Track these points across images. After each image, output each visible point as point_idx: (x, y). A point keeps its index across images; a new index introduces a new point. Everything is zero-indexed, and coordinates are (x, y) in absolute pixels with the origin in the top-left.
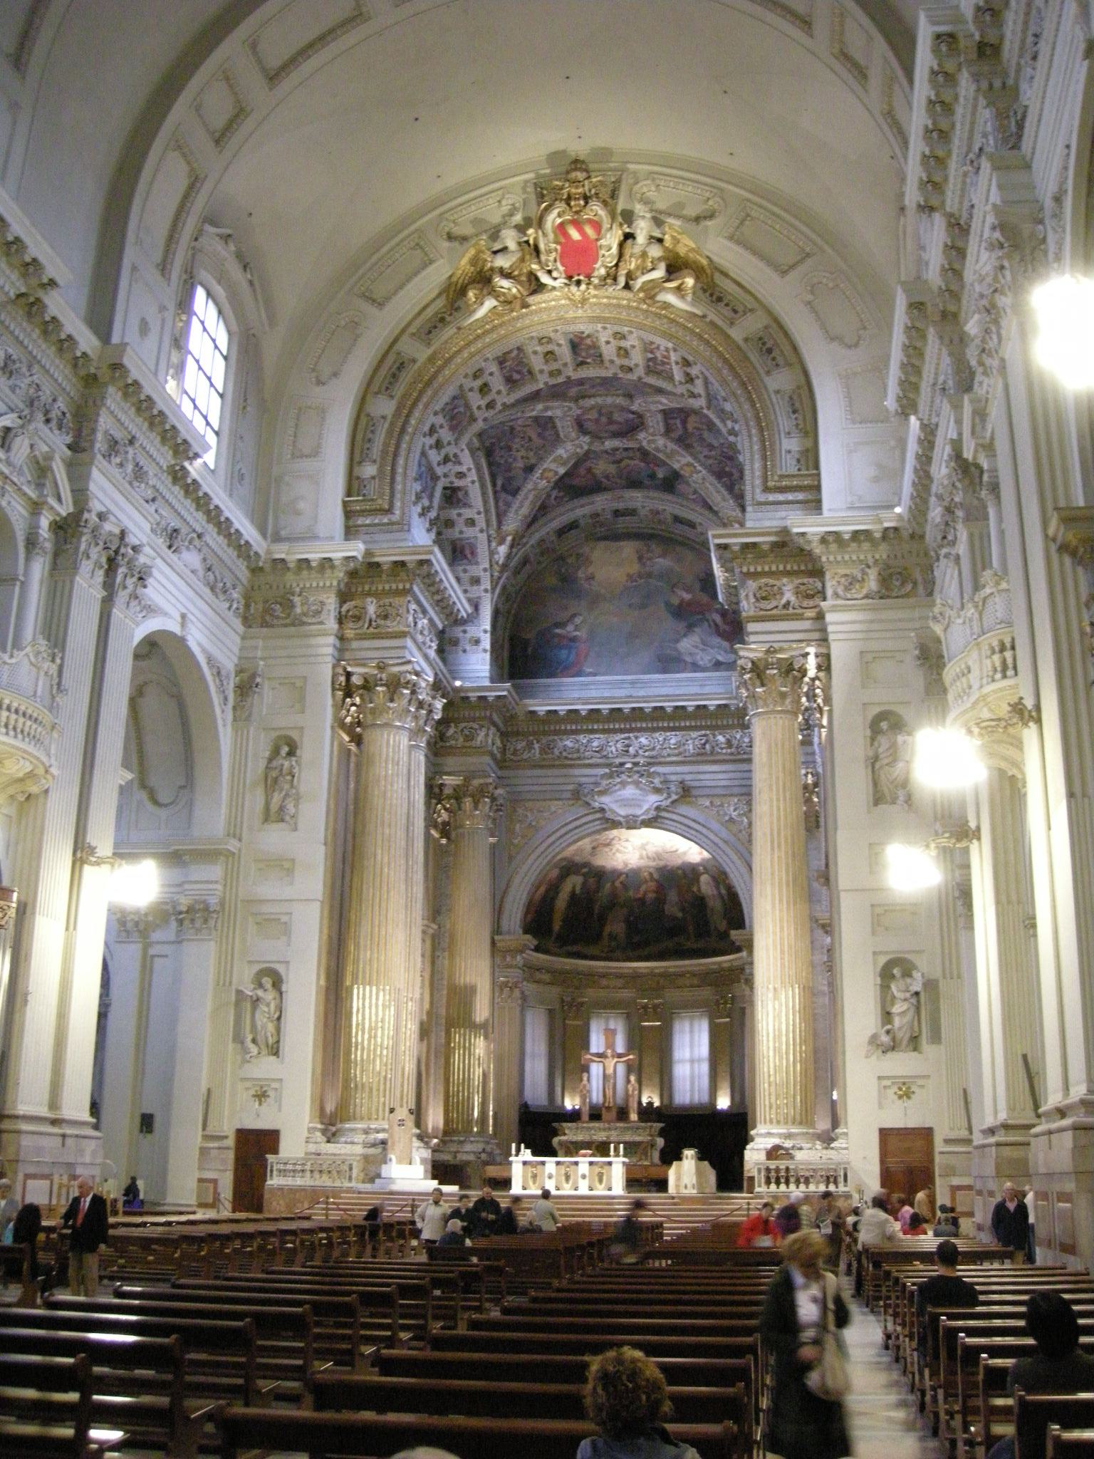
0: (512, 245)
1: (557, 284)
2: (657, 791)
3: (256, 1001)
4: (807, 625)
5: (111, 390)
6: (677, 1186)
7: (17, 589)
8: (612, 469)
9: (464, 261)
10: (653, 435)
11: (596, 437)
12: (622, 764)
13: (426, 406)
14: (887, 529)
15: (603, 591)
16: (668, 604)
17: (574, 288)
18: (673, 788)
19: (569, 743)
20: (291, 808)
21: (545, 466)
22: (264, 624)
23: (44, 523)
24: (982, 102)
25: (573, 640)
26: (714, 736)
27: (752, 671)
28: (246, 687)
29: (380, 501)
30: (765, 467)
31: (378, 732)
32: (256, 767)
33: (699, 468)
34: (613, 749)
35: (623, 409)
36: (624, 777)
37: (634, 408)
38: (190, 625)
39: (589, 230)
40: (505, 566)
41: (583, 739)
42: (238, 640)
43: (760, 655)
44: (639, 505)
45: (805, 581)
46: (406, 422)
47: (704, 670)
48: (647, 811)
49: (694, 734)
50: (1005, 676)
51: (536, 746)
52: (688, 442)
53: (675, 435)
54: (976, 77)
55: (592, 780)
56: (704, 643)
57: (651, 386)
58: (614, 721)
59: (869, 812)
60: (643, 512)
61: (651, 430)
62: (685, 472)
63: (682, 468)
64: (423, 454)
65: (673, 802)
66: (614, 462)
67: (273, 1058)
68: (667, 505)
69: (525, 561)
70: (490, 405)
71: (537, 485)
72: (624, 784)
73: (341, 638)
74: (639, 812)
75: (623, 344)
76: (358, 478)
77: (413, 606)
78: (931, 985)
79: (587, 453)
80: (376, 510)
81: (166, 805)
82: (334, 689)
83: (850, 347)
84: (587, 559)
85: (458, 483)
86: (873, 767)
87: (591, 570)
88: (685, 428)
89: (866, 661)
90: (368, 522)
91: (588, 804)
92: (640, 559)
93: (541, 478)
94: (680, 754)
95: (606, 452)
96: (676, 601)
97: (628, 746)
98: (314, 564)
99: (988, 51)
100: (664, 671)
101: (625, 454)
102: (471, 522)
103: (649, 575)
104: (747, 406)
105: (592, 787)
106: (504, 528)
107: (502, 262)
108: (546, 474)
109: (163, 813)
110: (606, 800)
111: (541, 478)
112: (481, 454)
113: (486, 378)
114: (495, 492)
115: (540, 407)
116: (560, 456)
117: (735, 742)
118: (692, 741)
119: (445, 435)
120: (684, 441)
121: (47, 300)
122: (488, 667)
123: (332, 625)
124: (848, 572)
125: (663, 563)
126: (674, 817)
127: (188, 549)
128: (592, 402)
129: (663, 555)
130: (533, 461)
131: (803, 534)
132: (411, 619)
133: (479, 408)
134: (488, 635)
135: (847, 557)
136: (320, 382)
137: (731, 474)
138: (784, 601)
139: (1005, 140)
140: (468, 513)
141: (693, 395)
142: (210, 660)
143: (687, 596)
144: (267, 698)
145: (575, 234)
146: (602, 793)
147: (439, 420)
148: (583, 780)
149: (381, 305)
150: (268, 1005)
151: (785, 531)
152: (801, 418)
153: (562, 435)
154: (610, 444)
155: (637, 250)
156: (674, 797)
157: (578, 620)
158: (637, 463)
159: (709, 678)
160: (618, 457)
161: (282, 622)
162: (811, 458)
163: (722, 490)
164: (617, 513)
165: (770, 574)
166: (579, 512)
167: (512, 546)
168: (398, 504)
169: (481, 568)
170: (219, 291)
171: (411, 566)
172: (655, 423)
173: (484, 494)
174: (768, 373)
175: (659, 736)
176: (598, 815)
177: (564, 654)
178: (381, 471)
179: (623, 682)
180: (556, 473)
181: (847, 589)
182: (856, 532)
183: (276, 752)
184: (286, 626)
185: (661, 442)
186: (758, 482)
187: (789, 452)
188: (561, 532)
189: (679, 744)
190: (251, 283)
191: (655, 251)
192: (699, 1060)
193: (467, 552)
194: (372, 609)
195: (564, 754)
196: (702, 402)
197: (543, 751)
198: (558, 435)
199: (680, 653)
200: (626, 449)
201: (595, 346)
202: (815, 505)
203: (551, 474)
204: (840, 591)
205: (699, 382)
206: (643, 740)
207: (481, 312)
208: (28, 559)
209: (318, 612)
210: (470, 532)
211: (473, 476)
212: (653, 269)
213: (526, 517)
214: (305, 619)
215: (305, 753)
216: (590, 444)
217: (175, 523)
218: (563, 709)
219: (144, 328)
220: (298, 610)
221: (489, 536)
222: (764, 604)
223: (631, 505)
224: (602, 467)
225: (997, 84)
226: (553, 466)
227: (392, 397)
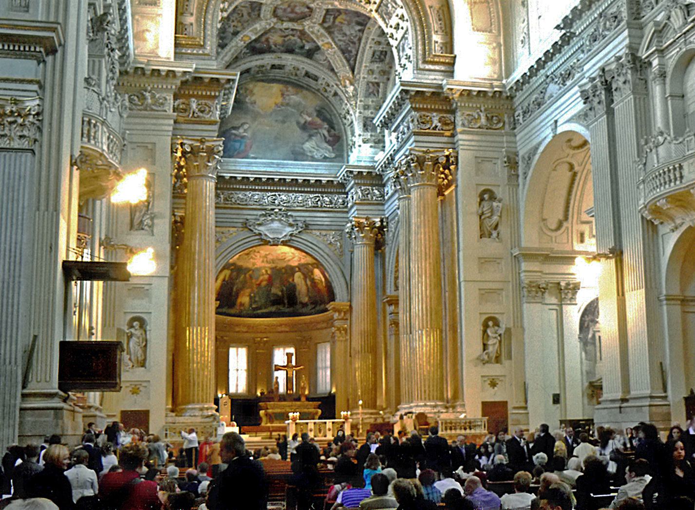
2: (291, 225)
4: (445, 139)
8: (280, 40)
12: (273, 210)
14: (496, 91)
15: (261, 111)
16: (298, 123)
18: (300, 225)
19: (240, 196)
20: (147, 221)
25: (243, 137)
27: (417, 161)
29: (198, 40)
30: (424, 49)
33: (334, 46)
34: (266, 201)
43: (421, 154)
44: (289, 63)
45: (445, 115)
49: (312, 196)
51: (222, 196)
52: (333, 30)
53: (326, 25)
55: (254, 217)
56: (318, 146)
58: (268, 185)
60: (287, 69)
61: (314, 20)
63: (323, 45)
66: (282, 37)
71: (238, 43)
72: (273, 220)
73: (175, 122)
76: (182, 23)
79: (270, 30)
80: (195, 45)
84: (252, 91)
87: (253, 98)
88: (334, 22)
89: (480, 161)
92: (283, 95)
93: (241, 40)
94: (303, 206)
95: (281, 30)
96: (303, 121)
97: (275, 200)
98: (163, 74)
100: (296, 160)
101: (291, 32)
103: (288, 104)
105: (253, 221)
108: (244, 38)
111: (241, 40)
116: (256, 29)
117: (334, 202)
118: (310, 199)
120: (329, 31)
123: (172, 111)
124: (470, 113)
125: (295, 98)
129: (296, 94)
130: (239, 29)
131: (452, 89)
137: (351, 52)
138: (434, 125)
143: (309, 119)
146: (260, 225)
148: (249, 217)
151: (440, 87)
152: (443, 23)
153: (262, 16)
154: (286, 25)
156: (300, 230)
157: (246, 126)
160: (287, 32)
161: (138, 107)
162: (449, 45)
163: (344, 61)
164: (273, 67)
165: (427, 110)
166: (254, 64)
171: (223, 82)
177: (237, 145)
178: (198, 20)
179: (273, 163)
180: (250, 38)
181: (470, 122)
182: (479, 92)
184: (140, 110)
185: (317, 27)
186: (420, 57)
187: (437, 42)
189: (303, 201)
194: (194, 106)
195: (238, 202)
196: (374, 7)
197: (225, 199)
198: (259, 15)
200: (293, 30)
202: (450, 73)
203: (246, 39)
204: (466, 122)
214: (154, 107)
216: (275, 24)
220: (150, 101)
222: (423, 126)
223: (283, 63)
224: (275, 39)
226: (250, 34)
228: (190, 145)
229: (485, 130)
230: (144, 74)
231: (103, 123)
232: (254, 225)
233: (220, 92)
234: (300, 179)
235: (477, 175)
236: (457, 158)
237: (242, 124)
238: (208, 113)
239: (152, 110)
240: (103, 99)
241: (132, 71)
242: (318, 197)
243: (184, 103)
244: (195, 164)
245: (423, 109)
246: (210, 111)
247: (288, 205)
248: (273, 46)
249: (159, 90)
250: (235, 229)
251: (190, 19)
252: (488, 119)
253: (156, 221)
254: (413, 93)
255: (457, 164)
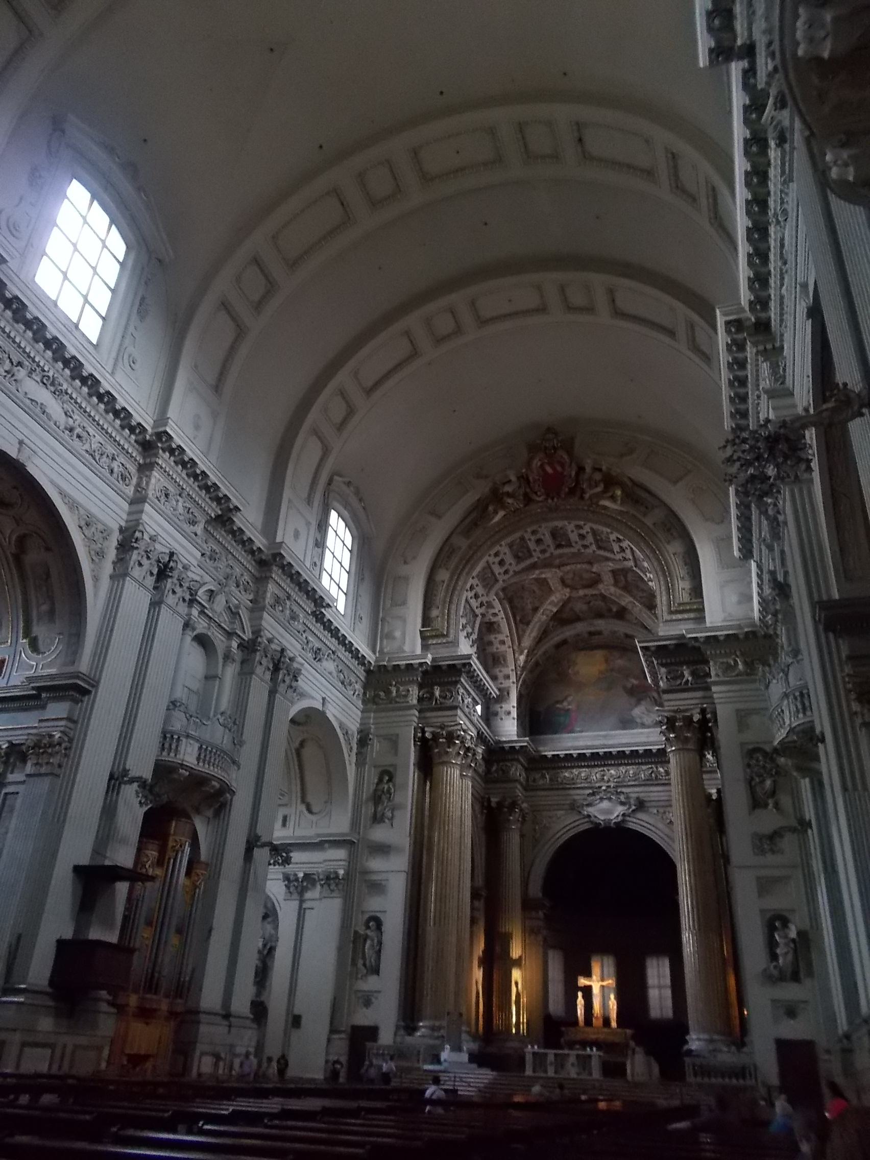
0: (513, 478)
1: (540, 499)
2: (622, 804)
3: (366, 938)
4: (699, 694)
5: (275, 568)
6: (633, 1075)
7: (217, 682)
8: (585, 607)
9: (487, 490)
10: (607, 585)
11: (573, 588)
12: (600, 787)
13: (468, 574)
16: (625, 688)
17: (550, 501)
18: (632, 802)
19: (566, 774)
20: (389, 814)
21: (545, 607)
22: (375, 703)
23: (234, 644)
24: (761, 359)
25: (568, 710)
26: (657, 768)
28: (364, 741)
31: (441, 767)
32: (368, 789)
33: (637, 604)
35: (587, 571)
36: (601, 795)
37: (594, 570)
38: (327, 704)
39: (559, 469)
40: (524, 668)
41: (576, 772)
42: (359, 713)
43: (672, 714)
45: (698, 667)
46: (456, 583)
47: (649, 727)
48: (618, 816)
49: (644, 767)
50: (804, 714)
51: (547, 776)
54: (755, 344)
55: (583, 797)
56: (649, 711)
57: (602, 556)
59: (750, 814)
61: (605, 583)
62: (629, 607)
64: (467, 601)
65: (633, 811)
66: (585, 603)
67: (375, 977)
68: (620, 628)
69: (537, 664)
70: (506, 572)
71: (540, 618)
72: (602, 799)
74: (612, 817)
75: (581, 532)
77: (461, 691)
78: (801, 934)
79: (569, 599)
81: (316, 814)
82: (415, 741)
83: (718, 523)
85: (494, 619)
86: (750, 783)
88: (626, 581)
90: (434, 642)
91: (580, 812)
92: (607, 661)
95: (580, 598)
96: (629, 685)
97: (603, 775)
98: (403, 667)
99: (763, 327)
100: (624, 728)
102: (503, 642)
104: (656, 564)
106: (522, 645)
107: (508, 489)
109: (314, 818)
110: (591, 810)
111: (543, 614)
112: (505, 602)
113: (501, 556)
114: (516, 624)
115: (537, 572)
116: (553, 601)
119: (480, 590)
120: (626, 588)
121: (235, 519)
122: (516, 728)
123: (415, 702)
124: (725, 660)
125: (620, 662)
126: (635, 820)
127: (327, 659)
128: (568, 568)
130: (537, 605)
132: (460, 698)
133: (499, 574)
134: (516, 709)
135: (723, 652)
136: (405, 563)
138: (684, 680)
139: (776, 380)
140: (501, 637)
141: (625, 559)
142: (341, 725)
143: (635, 682)
144: (376, 746)
145: (549, 470)
146: (589, 805)
147: (475, 582)
149: (439, 517)
150: (373, 940)
154: (581, 593)
155: (586, 476)
156: (634, 807)
157: (570, 699)
158: (600, 603)
159: (652, 732)
161: (385, 702)
162: (697, 591)
164: (591, 634)
167: (527, 656)
168: (452, 631)
169: (510, 669)
170: (346, 513)
172: (608, 578)
173: (509, 624)
174: (669, 543)
175: (622, 769)
176: (587, 820)
177: (562, 719)
180: (551, 611)
182: (728, 635)
183: (380, 780)
185: (612, 589)
186: (665, 608)
188: (558, 646)
190: (364, 508)
191: (598, 476)
192: (665, 987)
193: (501, 659)
195: (564, 781)
196: (631, 563)
197: (551, 780)
199: (633, 717)
200: (592, 595)
201: (565, 535)
202: (701, 619)
203: (548, 612)
204: (720, 674)
205: (628, 551)
206: (612, 772)
207: (497, 518)
208: (223, 666)
209: (406, 696)
210: (503, 648)
211: (502, 614)
212: (596, 486)
213: (535, 638)
214: (398, 700)
215: (398, 779)
216: (571, 592)
217: (317, 645)
218: (562, 753)
219: (297, 535)
220: (394, 694)
221: (513, 650)
222: (673, 682)
223: (598, 628)
224: (580, 607)
225: (769, 346)
226: (549, 607)
227: (447, 569)
228: (433, 733)
229: (745, 677)
230: (388, 671)
231: (188, 736)
232: (583, 805)
233: (460, 676)
234: (627, 750)
235: (740, 731)
236: (715, 714)
237: (566, 698)
238: (451, 698)
239: (396, 702)
240: (191, 716)
241: (376, 669)
242: (652, 768)
243: (427, 692)
244: (436, 750)
245: (671, 664)
246: (452, 696)
247: (618, 780)
248: (581, 615)
249: (403, 684)
250: (562, 812)
251: (434, 613)
252: (745, 663)
253: (396, 813)
254: (653, 649)
255: (716, 721)
